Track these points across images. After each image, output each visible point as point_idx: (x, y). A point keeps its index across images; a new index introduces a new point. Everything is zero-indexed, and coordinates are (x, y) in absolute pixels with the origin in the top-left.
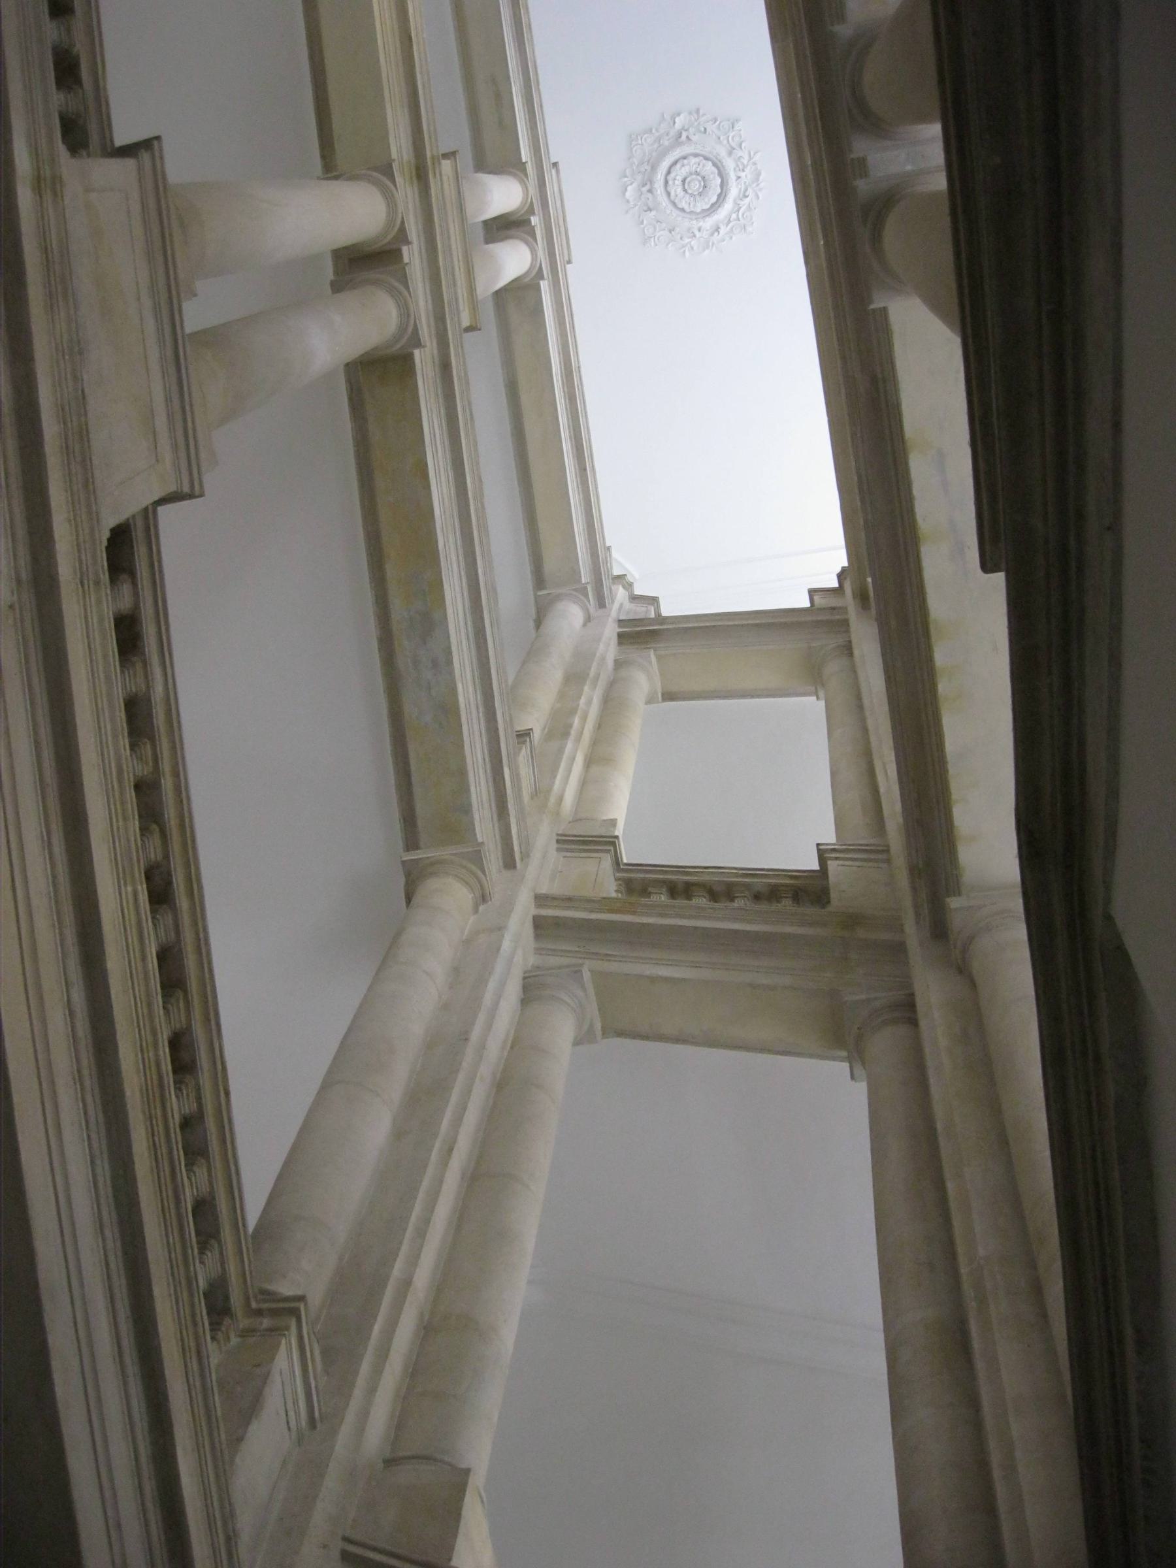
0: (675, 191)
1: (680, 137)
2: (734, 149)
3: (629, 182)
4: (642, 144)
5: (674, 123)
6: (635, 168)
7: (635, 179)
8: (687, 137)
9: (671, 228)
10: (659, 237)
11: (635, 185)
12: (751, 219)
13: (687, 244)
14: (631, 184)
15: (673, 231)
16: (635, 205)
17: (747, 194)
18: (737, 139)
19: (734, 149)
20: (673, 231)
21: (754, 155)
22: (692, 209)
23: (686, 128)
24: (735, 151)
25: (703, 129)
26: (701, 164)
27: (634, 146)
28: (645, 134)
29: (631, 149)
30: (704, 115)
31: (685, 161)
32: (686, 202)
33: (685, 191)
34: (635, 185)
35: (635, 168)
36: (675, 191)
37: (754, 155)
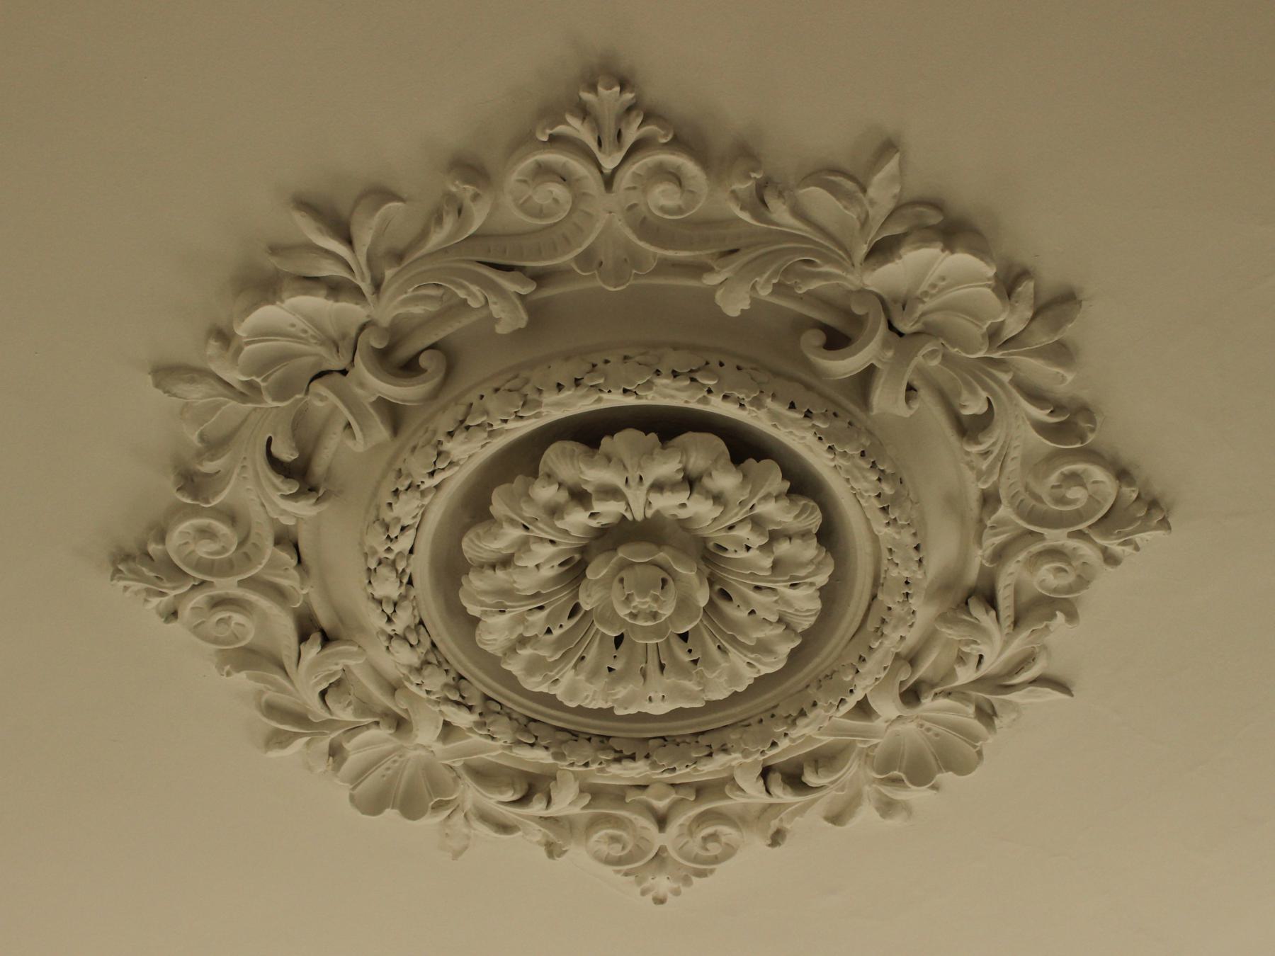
0: (524, 545)
1: (837, 341)
2: (991, 602)
3: (329, 269)
4: (609, 181)
5: (883, 250)
6: (437, 238)
7: (377, 286)
8: (867, 377)
9: (324, 618)
10: (219, 603)
11: (352, 312)
12: (716, 860)
13: (330, 724)
14: (335, 288)
15: (327, 639)
16: (250, 392)
17: (810, 778)
18: (1047, 578)
19: (991, 602)
20: (327, 639)
21: (1035, 682)
22: (514, 667)
23: (906, 327)
24: (985, 618)
25: (973, 407)
26: (783, 548)
27: (553, 139)
28: (678, 143)
29: (523, 141)
30: (1062, 353)
31: (726, 480)
32: (520, 620)
33: (574, 570)
34: (352, 312)
35: (437, 238)
36: (524, 545)
37: (1035, 682)
